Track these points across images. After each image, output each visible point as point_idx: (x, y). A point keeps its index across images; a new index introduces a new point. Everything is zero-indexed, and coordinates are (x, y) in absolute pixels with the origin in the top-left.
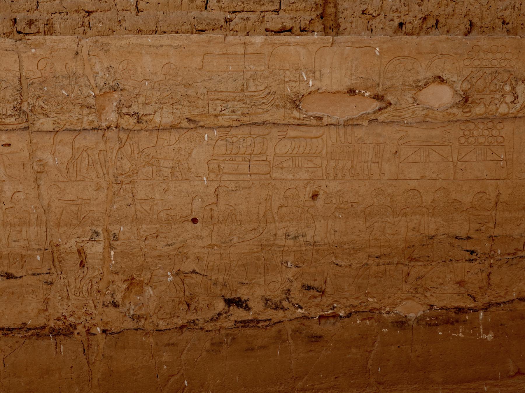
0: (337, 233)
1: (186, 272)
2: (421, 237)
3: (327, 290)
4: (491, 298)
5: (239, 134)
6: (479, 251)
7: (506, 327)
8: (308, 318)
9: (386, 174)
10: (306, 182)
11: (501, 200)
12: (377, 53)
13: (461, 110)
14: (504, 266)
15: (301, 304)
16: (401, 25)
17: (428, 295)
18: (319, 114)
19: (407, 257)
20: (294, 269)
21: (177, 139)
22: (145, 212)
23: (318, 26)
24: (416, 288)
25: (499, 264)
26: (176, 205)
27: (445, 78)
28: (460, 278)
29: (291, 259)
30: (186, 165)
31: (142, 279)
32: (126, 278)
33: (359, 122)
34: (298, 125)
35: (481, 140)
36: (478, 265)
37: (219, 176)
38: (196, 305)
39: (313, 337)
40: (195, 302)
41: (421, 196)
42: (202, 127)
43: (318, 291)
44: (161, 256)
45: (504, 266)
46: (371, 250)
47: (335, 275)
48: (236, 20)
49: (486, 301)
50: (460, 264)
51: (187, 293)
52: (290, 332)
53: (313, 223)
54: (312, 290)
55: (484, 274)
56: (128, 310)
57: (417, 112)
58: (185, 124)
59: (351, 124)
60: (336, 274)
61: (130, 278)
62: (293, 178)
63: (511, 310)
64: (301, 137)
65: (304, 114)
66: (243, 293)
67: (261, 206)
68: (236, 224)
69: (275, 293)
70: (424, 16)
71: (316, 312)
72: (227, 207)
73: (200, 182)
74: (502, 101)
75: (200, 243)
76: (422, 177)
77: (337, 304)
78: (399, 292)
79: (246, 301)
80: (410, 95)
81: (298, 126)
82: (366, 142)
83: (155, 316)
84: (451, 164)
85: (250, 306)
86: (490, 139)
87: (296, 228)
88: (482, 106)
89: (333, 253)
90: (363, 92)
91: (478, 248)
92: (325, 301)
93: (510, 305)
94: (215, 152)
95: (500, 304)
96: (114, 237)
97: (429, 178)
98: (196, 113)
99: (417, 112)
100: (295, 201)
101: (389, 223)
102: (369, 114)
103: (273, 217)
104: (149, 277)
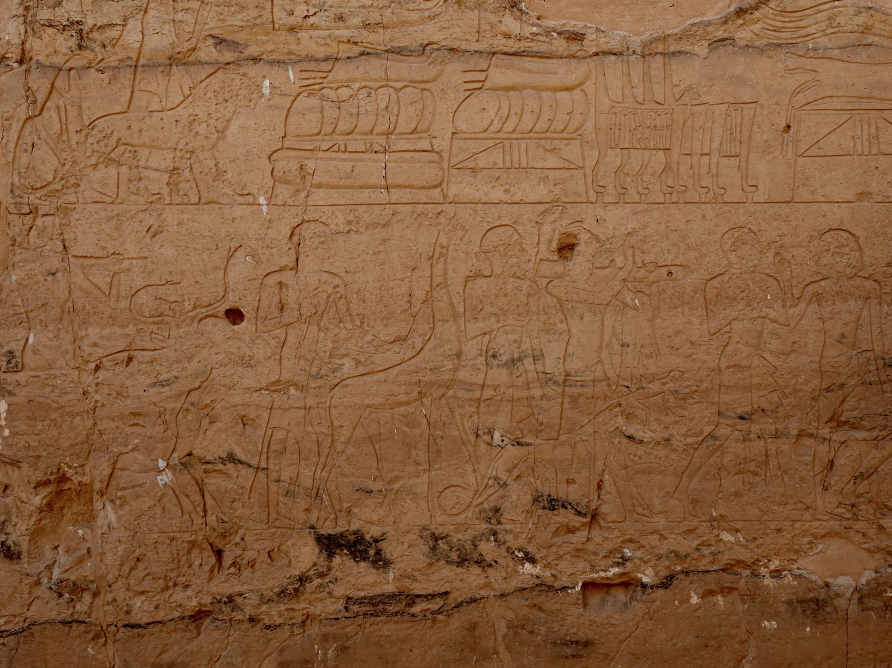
0: (630, 350)
1: (208, 458)
3: (603, 509)
5: (355, 80)
8: (551, 587)
9: (761, 187)
10: (542, 208)
15: (531, 549)
18: (575, 25)
21: (187, 92)
22: (96, 291)
24: (853, 506)
26: (183, 272)
29: (501, 422)
30: (212, 163)
31: (86, 479)
32: (40, 476)
33: (684, 46)
34: (515, 54)
37: (304, 194)
38: (238, 551)
39: (566, 644)
40: (237, 544)
41: (860, 249)
42: (255, 60)
43: (579, 513)
44: (140, 415)
46: (725, 398)
47: (626, 467)
51: (212, 519)
52: (502, 630)
53: (561, 322)
54: (562, 510)
56: (50, 567)
57: (841, 19)
58: (208, 52)
60: (629, 463)
61: (53, 477)
62: (505, 198)
64: (525, 87)
65: (533, 25)
66: (367, 519)
67: (418, 273)
68: (349, 326)
69: (459, 519)
71: (574, 573)
72: (326, 276)
73: (249, 209)
75: (250, 379)
77: (633, 550)
78: (807, 515)
79: (377, 541)
81: (516, 59)
82: (703, 99)
83: (119, 583)
85: (388, 556)
87: (516, 337)
89: (620, 405)
92: (599, 540)
94: (291, 129)
96: (9, 362)
97: (880, 198)
98: (239, 23)
99: (841, 19)
100: (513, 261)
101: (773, 321)
102: (709, 24)
103: (452, 305)
104: (107, 472)
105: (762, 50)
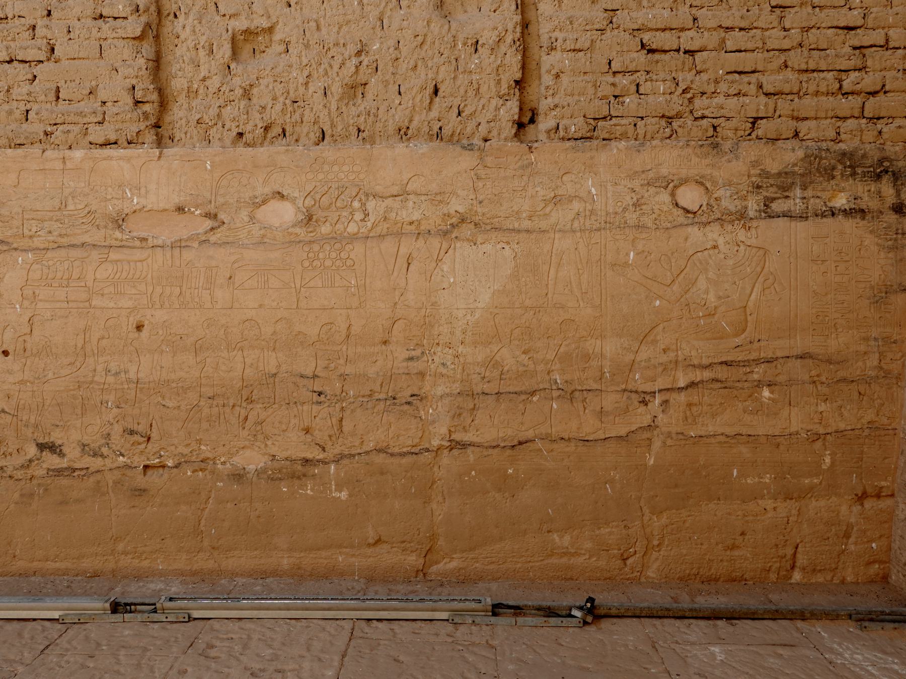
3: (152, 435)
4: (343, 448)
10: (129, 310)
11: (353, 332)
12: (209, 167)
14: (358, 410)
15: (123, 451)
16: (240, 135)
17: (269, 443)
18: (143, 234)
19: (244, 399)
20: (115, 410)
23: (150, 137)
27: (285, 194)
28: (306, 424)
29: (112, 398)
35: (328, 263)
42: (16, 249)
45: (358, 410)
48: (58, 133)
49: (337, 450)
50: (305, 407)
52: (111, 484)
55: (334, 420)
57: (253, 232)
59: (179, 245)
66: (57, 437)
71: (140, 461)
73: (12, 310)
75: (11, 379)
76: (261, 306)
80: (246, 213)
86: (338, 263)
88: (328, 224)
90: (192, 209)
91: (327, 389)
95: (354, 456)
99: (253, 232)
102: (199, 234)
105: (220, 245)
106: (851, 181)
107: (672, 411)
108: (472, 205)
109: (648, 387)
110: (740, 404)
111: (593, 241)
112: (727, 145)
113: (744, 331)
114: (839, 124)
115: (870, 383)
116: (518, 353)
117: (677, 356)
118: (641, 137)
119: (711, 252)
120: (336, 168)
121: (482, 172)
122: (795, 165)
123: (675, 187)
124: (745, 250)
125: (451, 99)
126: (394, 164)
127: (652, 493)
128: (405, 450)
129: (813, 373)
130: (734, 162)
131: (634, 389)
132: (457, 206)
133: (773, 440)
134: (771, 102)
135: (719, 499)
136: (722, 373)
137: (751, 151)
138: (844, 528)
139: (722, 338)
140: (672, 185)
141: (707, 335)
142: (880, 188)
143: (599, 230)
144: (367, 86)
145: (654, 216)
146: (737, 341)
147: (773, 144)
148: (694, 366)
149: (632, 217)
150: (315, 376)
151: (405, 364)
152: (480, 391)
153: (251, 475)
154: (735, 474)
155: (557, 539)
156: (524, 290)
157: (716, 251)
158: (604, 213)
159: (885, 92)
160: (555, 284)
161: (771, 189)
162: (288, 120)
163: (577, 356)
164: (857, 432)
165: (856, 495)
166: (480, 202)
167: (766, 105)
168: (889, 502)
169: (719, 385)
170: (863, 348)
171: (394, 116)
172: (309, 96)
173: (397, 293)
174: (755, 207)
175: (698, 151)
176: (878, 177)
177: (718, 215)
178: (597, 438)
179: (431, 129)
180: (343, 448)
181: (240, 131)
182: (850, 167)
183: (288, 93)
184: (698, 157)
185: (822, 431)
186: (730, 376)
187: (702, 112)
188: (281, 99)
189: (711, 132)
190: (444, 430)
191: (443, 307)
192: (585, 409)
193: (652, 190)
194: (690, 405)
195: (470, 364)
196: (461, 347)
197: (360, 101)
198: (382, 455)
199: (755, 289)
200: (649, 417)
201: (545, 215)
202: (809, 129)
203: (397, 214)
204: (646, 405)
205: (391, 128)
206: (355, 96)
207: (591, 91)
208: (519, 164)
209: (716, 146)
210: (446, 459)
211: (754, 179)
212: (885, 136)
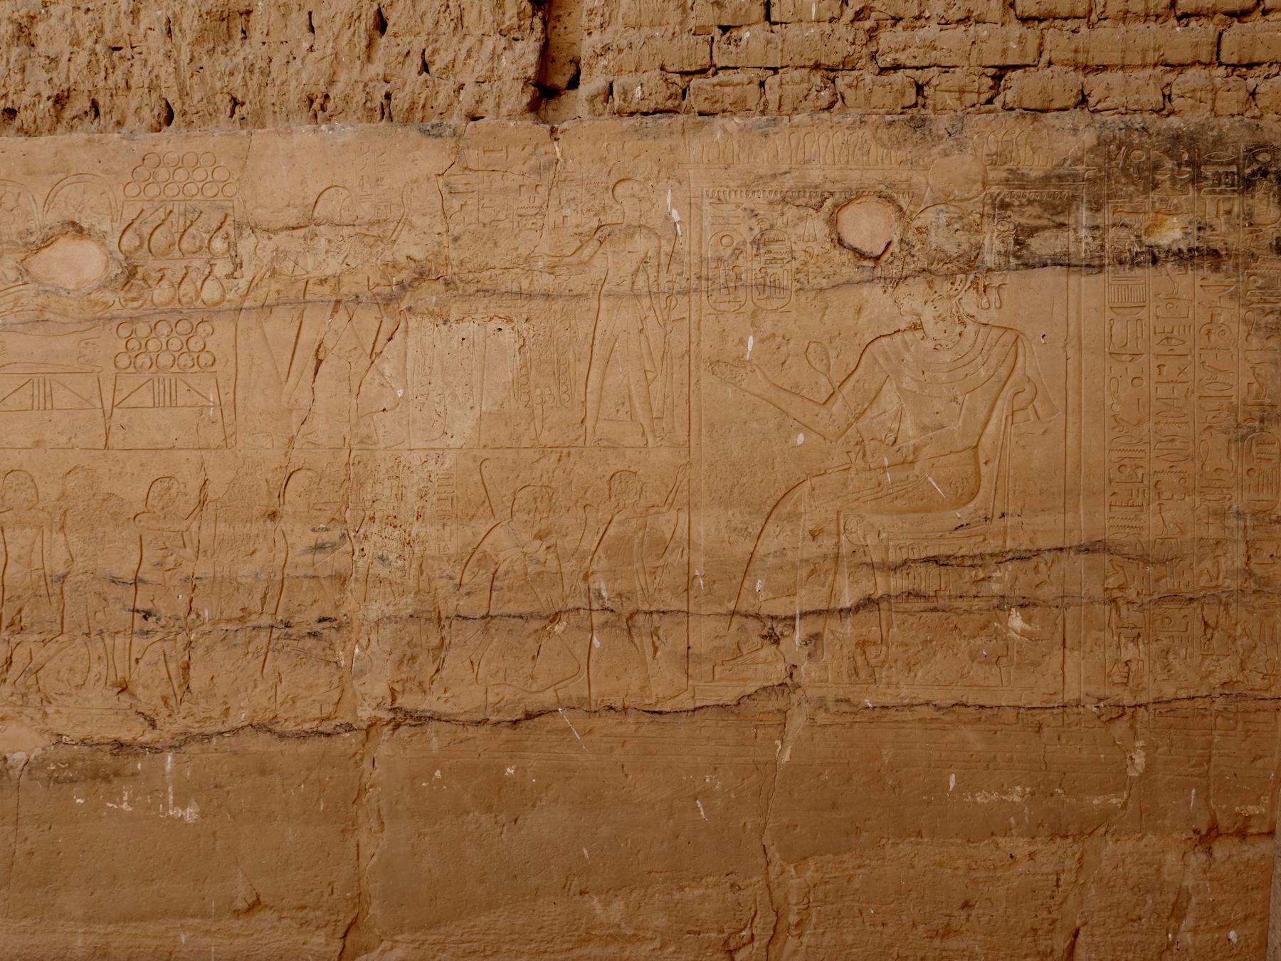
2: (35, 576)
6: (163, 611)
7: (228, 793)
11: (211, 495)
13: (122, 294)
17: (50, 710)
24: (23, 695)
25: (207, 643)
27: (85, 225)
36: (159, 644)
49: (178, 725)
55: (173, 667)
57: (24, 301)
63: (235, 753)
70: (56, 92)
74: (206, 273)
76: (37, 444)
80: (11, 263)
84: (99, 413)
86: (185, 360)
88: (165, 284)
91: (161, 606)
93: (233, 739)
99: (24, 301)
106: (1192, 193)
107: (827, 656)
108: (440, 244)
109: (780, 607)
110: (964, 643)
111: (675, 315)
112: (942, 123)
113: (973, 495)
114: (1169, 77)
115: (1227, 604)
116: (525, 537)
117: (838, 544)
118: (772, 107)
119: (908, 336)
120: (181, 175)
121: (459, 181)
122: (1079, 160)
123: (838, 207)
124: (977, 333)
125: (408, 39)
126: (293, 165)
127: (785, 820)
128: (307, 727)
129: (1112, 582)
130: (955, 156)
131: (752, 611)
132: (410, 247)
133: (1030, 718)
134: (1031, 34)
135: (919, 834)
136: (927, 580)
137: (991, 132)
138: (1172, 898)
139: (927, 510)
140: (832, 204)
141: (899, 503)
142: (1251, 207)
143: (686, 292)
144: (252, 17)
145: (795, 264)
146: (960, 515)
147: (1035, 119)
148: (872, 565)
149: (750, 267)
150: (137, 582)
151: (308, 558)
152: (452, 612)
153: (17, 773)
154: (952, 785)
155: (598, 908)
156: (538, 411)
157: (919, 334)
158: (695, 260)
159: (1265, 12)
160: (600, 399)
161: (1030, 210)
162: (101, 84)
163: (642, 543)
164: (1199, 703)
165: (1197, 832)
166: (456, 239)
167: (1021, 40)
168: (1264, 846)
169: (921, 604)
170: (1213, 532)
171: (298, 72)
172: (141, 37)
173: (295, 419)
174: (998, 246)
175: (883, 134)
176: (1247, 184)
177: (924, 263)
178: (679, 707)
179: (369, 97)
180: (189, 721)
181: (9, 105)
182: (1189, 164)
183: (102, 31)
184: (884, 145)
185: (1128, 700)
186: (943, 587)
187: (892, 56)
188: (89, 43)
189: (911, 97)
190: (381, 689)
191: (382, 445)
192: (656, 649)
193: (791, 212)
194: (862, 644)
195: (433, 558)
196: (416, 524)
197: (238, 47)
198: (264, 737)
199: (996, 412)
200: (781, 666)
201: (581, 263)
202: (1108, 88)
203: (296, 264)
204: (777, 642)
205: (294, 97)
206: (230, 36)
207: (674, 17)
208: (531, 163)
209: (919, 124)
210: (385, 746)
211: (994, 190)
212: (1263, 101)
